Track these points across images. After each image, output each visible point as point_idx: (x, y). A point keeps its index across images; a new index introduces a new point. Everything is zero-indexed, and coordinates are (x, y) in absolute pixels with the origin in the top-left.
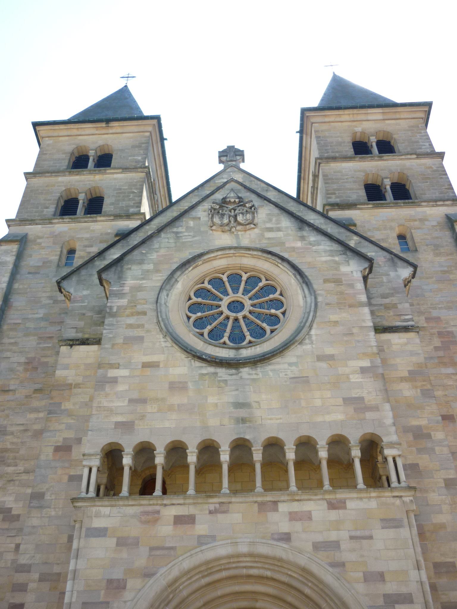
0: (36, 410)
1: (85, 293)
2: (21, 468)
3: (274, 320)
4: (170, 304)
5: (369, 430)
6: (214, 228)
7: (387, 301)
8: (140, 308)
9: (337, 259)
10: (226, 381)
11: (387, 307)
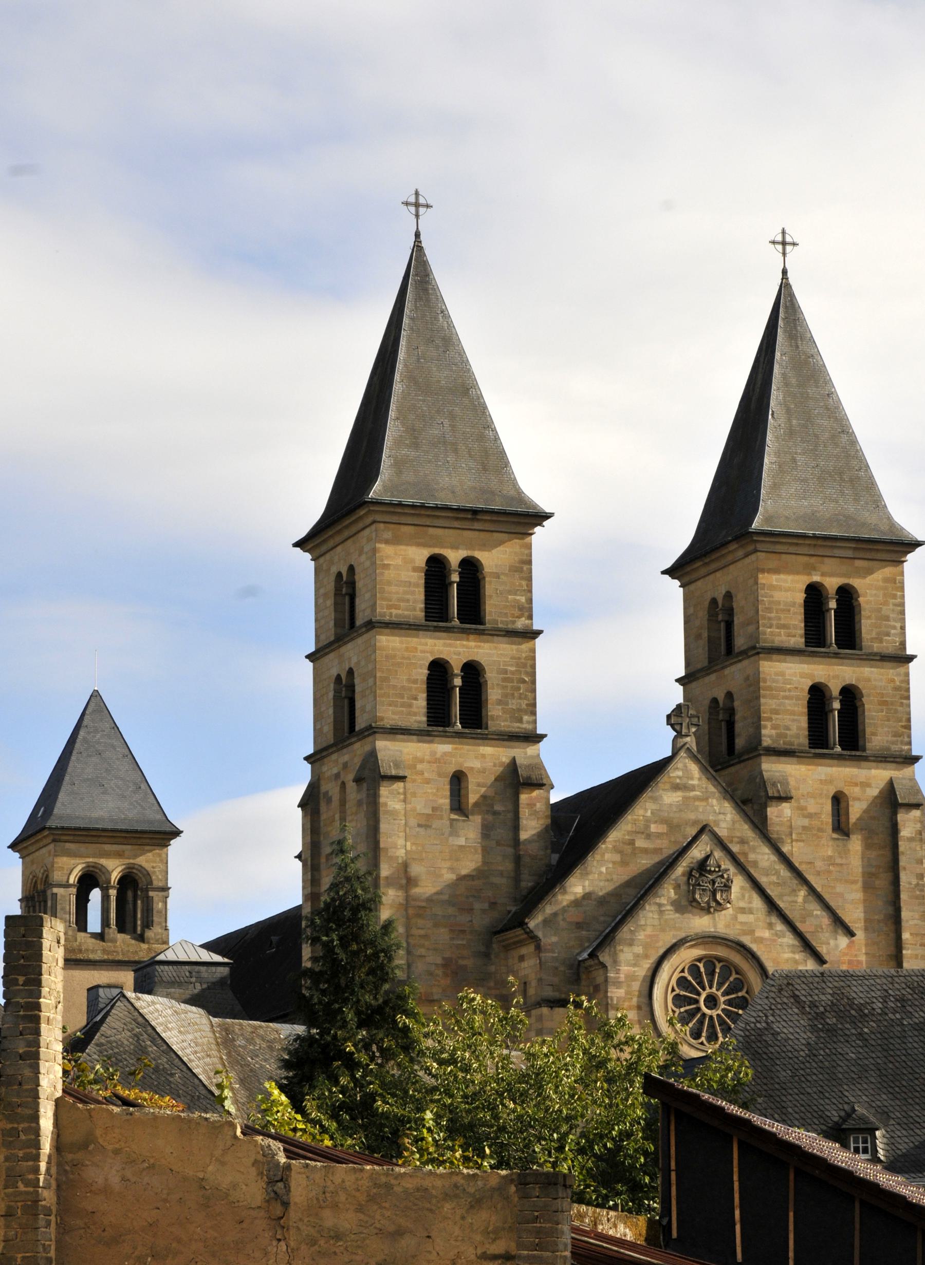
1: (554, 939)
6: (694, 904)
9: (797, 956)
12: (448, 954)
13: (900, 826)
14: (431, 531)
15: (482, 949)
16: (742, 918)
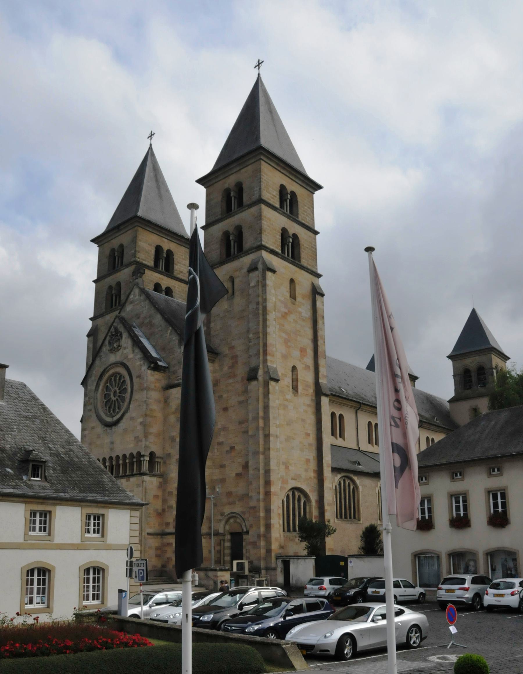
5: (138, 450)
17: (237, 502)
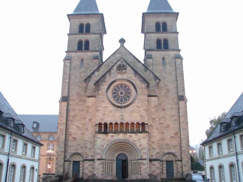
0: (80, 105)
2: (79, 118)
3: (129, 97)
4: (109, 93)
7: (153, 89)
8: (103, 94)
10: (119, 111)
11: (153, 90)
12: (78, 92)
13: (176, 62)
14: (81, 19)
15: (85, 90)
16: (129, 75)
17: (172, 148)
